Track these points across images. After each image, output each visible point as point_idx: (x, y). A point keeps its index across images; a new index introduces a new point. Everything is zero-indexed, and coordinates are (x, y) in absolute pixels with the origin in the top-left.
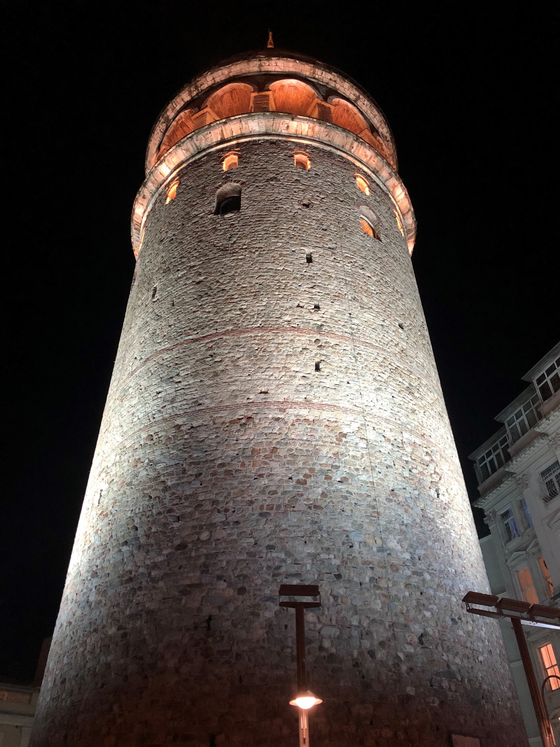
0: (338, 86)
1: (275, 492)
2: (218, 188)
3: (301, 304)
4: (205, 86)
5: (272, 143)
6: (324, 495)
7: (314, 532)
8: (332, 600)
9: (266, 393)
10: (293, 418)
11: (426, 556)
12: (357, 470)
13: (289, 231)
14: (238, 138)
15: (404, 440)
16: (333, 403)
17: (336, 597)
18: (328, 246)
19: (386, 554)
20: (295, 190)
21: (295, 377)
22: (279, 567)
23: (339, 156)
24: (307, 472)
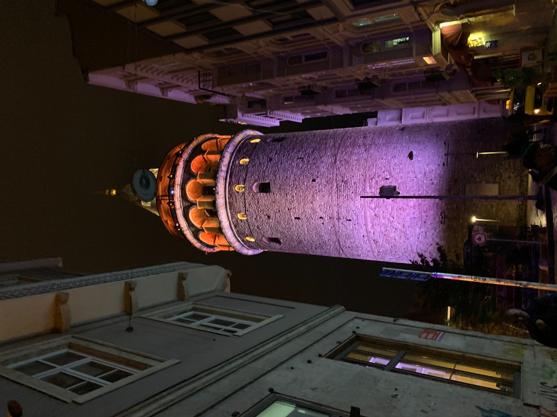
0: (179, 196)
1: (400, 236)
2: (266, 243)
3: (322, 223)
4: (200, 245)
5: (235, 227)
6: (399, 223)
7: (412, 227)
8: (432, 225)
9: (363, 236)
10: (372, 229)
11: (413, 191)
12: (388, 212)
13: (286, 224)
14: (236, 237)
15: (370, 191)
16: (363, 217)
17: (431, 224)
18: (288, 211)
19: (415, 207)
20: (261, 220)
21: (355, 228)
22: (424, 237)
23: (228, 199)
24: (392, 227)
